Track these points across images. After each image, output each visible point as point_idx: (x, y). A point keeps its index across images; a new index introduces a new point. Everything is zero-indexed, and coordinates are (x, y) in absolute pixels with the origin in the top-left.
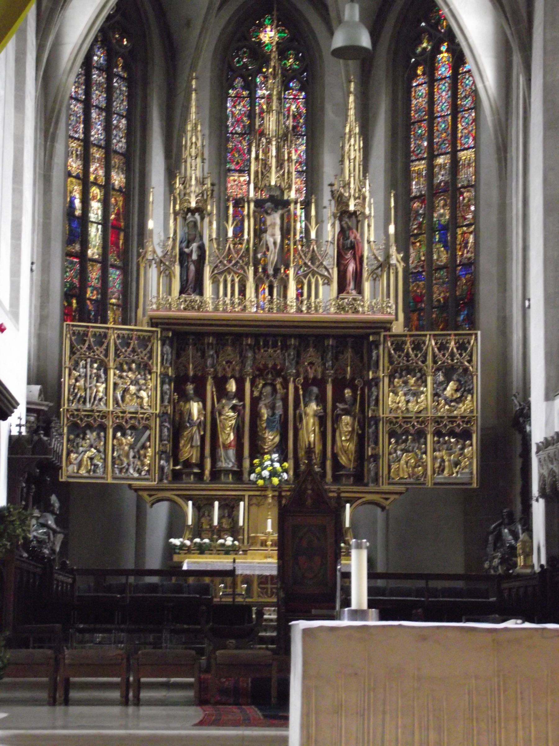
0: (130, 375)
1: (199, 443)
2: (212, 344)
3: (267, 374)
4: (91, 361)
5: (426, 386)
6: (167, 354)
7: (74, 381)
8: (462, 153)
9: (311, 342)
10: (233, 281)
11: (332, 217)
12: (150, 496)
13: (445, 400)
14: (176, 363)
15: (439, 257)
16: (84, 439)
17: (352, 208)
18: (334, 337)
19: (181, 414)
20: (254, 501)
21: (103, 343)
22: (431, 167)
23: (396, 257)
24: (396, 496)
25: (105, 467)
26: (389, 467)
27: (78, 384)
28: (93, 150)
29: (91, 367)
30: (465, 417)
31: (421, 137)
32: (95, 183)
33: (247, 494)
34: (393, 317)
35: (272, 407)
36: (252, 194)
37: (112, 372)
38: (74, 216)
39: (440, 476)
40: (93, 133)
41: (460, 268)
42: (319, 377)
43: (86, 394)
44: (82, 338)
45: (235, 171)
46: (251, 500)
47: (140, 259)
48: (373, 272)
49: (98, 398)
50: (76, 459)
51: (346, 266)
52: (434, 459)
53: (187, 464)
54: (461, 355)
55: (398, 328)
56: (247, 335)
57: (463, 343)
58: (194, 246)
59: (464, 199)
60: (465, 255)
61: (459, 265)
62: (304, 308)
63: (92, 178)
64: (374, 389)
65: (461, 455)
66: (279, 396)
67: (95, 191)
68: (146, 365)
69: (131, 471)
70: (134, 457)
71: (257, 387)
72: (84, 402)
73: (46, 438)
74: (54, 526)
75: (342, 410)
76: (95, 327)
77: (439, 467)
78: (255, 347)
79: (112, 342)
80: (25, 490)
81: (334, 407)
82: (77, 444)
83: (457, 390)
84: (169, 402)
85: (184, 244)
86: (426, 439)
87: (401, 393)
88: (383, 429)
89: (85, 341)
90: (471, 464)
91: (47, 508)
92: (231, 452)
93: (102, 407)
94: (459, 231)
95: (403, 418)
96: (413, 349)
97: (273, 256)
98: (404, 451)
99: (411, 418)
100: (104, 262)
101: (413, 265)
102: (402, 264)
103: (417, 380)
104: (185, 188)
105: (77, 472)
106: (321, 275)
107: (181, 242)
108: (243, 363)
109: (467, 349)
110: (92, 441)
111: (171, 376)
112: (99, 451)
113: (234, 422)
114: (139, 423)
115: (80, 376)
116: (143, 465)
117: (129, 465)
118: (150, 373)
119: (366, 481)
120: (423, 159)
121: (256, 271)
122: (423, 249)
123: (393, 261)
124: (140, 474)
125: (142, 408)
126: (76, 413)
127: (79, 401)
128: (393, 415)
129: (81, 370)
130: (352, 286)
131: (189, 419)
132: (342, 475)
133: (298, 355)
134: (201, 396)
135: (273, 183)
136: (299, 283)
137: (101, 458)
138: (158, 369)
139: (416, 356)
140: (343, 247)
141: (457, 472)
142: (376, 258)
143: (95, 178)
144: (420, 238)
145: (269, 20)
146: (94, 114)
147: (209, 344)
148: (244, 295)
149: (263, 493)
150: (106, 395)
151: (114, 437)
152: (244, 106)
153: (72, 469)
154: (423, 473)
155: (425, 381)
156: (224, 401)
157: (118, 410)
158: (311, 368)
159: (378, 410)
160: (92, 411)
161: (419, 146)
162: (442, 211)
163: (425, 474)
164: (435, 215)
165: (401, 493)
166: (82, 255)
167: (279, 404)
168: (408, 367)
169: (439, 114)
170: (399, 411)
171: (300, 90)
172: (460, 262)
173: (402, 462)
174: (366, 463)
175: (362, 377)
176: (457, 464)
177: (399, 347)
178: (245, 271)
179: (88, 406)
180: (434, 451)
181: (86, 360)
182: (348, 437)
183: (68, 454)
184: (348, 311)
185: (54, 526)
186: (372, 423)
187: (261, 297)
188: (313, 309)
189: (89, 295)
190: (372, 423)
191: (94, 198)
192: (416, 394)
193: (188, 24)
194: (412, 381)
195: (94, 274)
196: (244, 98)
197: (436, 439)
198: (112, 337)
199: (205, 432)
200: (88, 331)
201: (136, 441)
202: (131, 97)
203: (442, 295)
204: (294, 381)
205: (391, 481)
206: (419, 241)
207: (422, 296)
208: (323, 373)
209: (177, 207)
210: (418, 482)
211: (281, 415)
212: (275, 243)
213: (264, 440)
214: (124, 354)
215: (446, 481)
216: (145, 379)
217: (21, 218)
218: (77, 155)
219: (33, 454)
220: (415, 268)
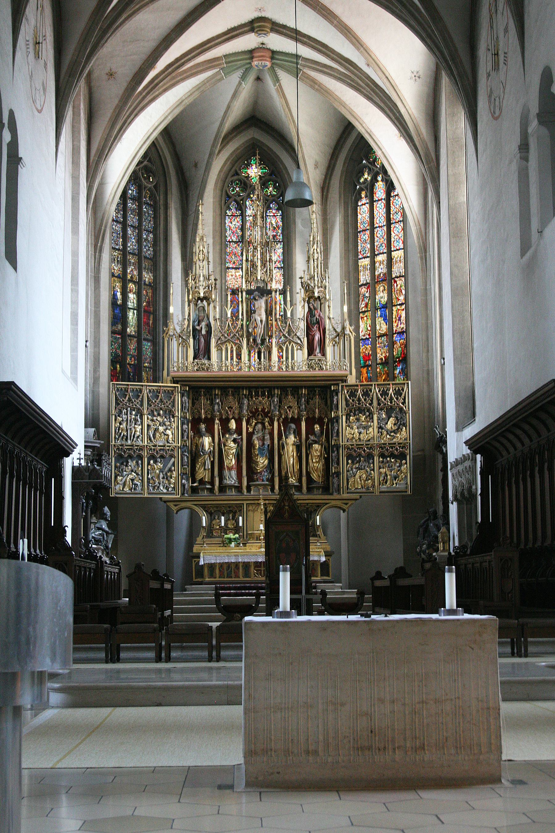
0: (159, 418)
1: (210, 467)
2: (218, 395)
3: (258, 415)
4: (131, 409)
5: (373, 422)
6: (186, 403)
7: (118, 424)
8: (395, 252)
9: (289, 392)
10: (232, 347)
11: (303, 301)
12: (176, 505)
13: (387, 432)
14: (192, 409)
15: (380, 327)
16: (126, 466)
17: (316, 295)
18: (305, 387)
19: (197, 446)
20: (250, 508)
21: (139, 396)
22: (373, 263)
23: (349, 329)
24: (353, 502)
25: (143, 486)
26: (348, 480)
27: (121, 426)
28: (130, 257)
29: (131, 414)
30: (401, 443)
32: (131, 281)
33: (245, 502)
34: (348, 372)
35: (263, 439)
36: (244, 287)
37: (146, 416)
38: (117, 305)
39: (384, 486)
40: (129, 245)
41: (395, 335)
42: (296, 417)
43: (127, 434)
44: (124, 392)
45: (233, 268)
46: (249, 506)
47: (165, 335)
48: (333, 339)
49: (136, 436)
50: (121, 480)
51: (314, 336)
52: (380, 473)
53: (202, 482)
54: (397, 399)
56: (243, 388)
57: (399, 389)
58: (203, 324)
59: (397, 285)
60: (399, 326)
61: (396, 333)
62: (284, 367)
63: (129, 277)
64: (335, 424)
65: (399, 471)
66: (267, 431)
67: (131, 286)
68: (170, 411)
69: (162, 488)
70: (163, 478)
71: (251, 425)
72: (126, 440)
73: (98, 468)
74: (107, 529)
75: (313, 441)
76: (133, 385)
77: (383, 480)
78: (249, 396)
79: (145, 395)
80: (85, 504)
81: (307, 438)
82: (122, 470)
83: (395, 424)
84: (188, 438)
85: (196, 323)
86: (373, 459)
87: (355, 427)
89: (126, 395)
90: (406, 477)
91: (102, 516)
92: (234, 473)
94: (394, 309)
95: (357, 445)
96: (362, 396)
97: (260, 331)
98: (359, 469)
99: (363, 445)
100: (139, 336)
101: (363, 333)
102: (354, 334)
103: (366, 417)
104: (195, 283)
105: (123, 490)
106: (295, 343)
107: (194, 322)
108: (241, 408)
109: (402, 394)
110: (133, 467)
111: (189, 419)
112: (137, 474)
113: (234, 451)
114: (166, 453)
115: (123, 420)
116: (170, 484)
117: (160, 484)
118: (173, 417)
119: (331, 490)
120: (368, 257)
121: (248, 340)
122: (369, 322)
123: (347, 332)
124: (168, 490)
125: (168, 442)
126: (120, 447)
127: (122, 438)
128: (349, 443)
129: (124, 416)
130: (318, 350)
131: (202, 449)
132: (313, 488)
133: (280, 401)
134: (210, 431)
135: (259, 278)
137: (140, 479)
138: (178, 413)
139: (365, 400)
140: (311, 322)
141: (396, 484)
142: (334, 329)
143: (131, 277)
144: (367, 314)
145: (254, 160)
147: (215, 395)
148: (240, 359)
149: (256, 502)
150: (142, 434)
151: (149, 464)
152: (238, 222)
153: (119, 487)
154: (372, 484)
155: (373, 418)
156: (227, 436)
157: (151, 444)
158: (289, 411)
159: (339, 440)
160: (132, 445)
161: (364, 248)
162: (382, 294)
163: (373, 486)
164: (377, 297)
165: (356, 499)
166: (123, 334)
167: (267, 437)
168: (359, 408)
169: (377, 225)
170: (354, 440)
171: (278, 210)
172: (396, 331)
173: (357, 476)
174: (331, 478)
175: (326, 416)
176: (395, 478)
177: (353, 394)
178: (240, 341)
179: (129, 442)
180: (380, 468)
181: (127, 409)
182: (317, 460)
183: (116, 477)
184: (315, 369)
185: (107, 529)
186: (335, 449)
187: (252, 359)
188: (290, 368)
189: (128, 360)
190: (335, 449)
191: (131, 291)
192: (366, 428)
193: (196, 165)
194: (363, 418)
195: (132, 346)
196: (238, 216)
197: (381, 459)
198: (145, 392)
199: (214, 458)
200: (128, 389)
201: (165, 466)
202: (156, 218)
203: (384, 355)
204: (278, 420)
205: (349, 491)
206: (366, 316)
207: (369, 355)
208: (298, 413)
209: (191, 297)
210: (368, 491)
211: (268, 445)
212: (261, 321)
213: (257, 463)
214: (154, 404)
215: (388, 490)
216: (170, 422)
217: (78, 309)
218: (118, 261)
219: (89, 479)
220: (364, 336)
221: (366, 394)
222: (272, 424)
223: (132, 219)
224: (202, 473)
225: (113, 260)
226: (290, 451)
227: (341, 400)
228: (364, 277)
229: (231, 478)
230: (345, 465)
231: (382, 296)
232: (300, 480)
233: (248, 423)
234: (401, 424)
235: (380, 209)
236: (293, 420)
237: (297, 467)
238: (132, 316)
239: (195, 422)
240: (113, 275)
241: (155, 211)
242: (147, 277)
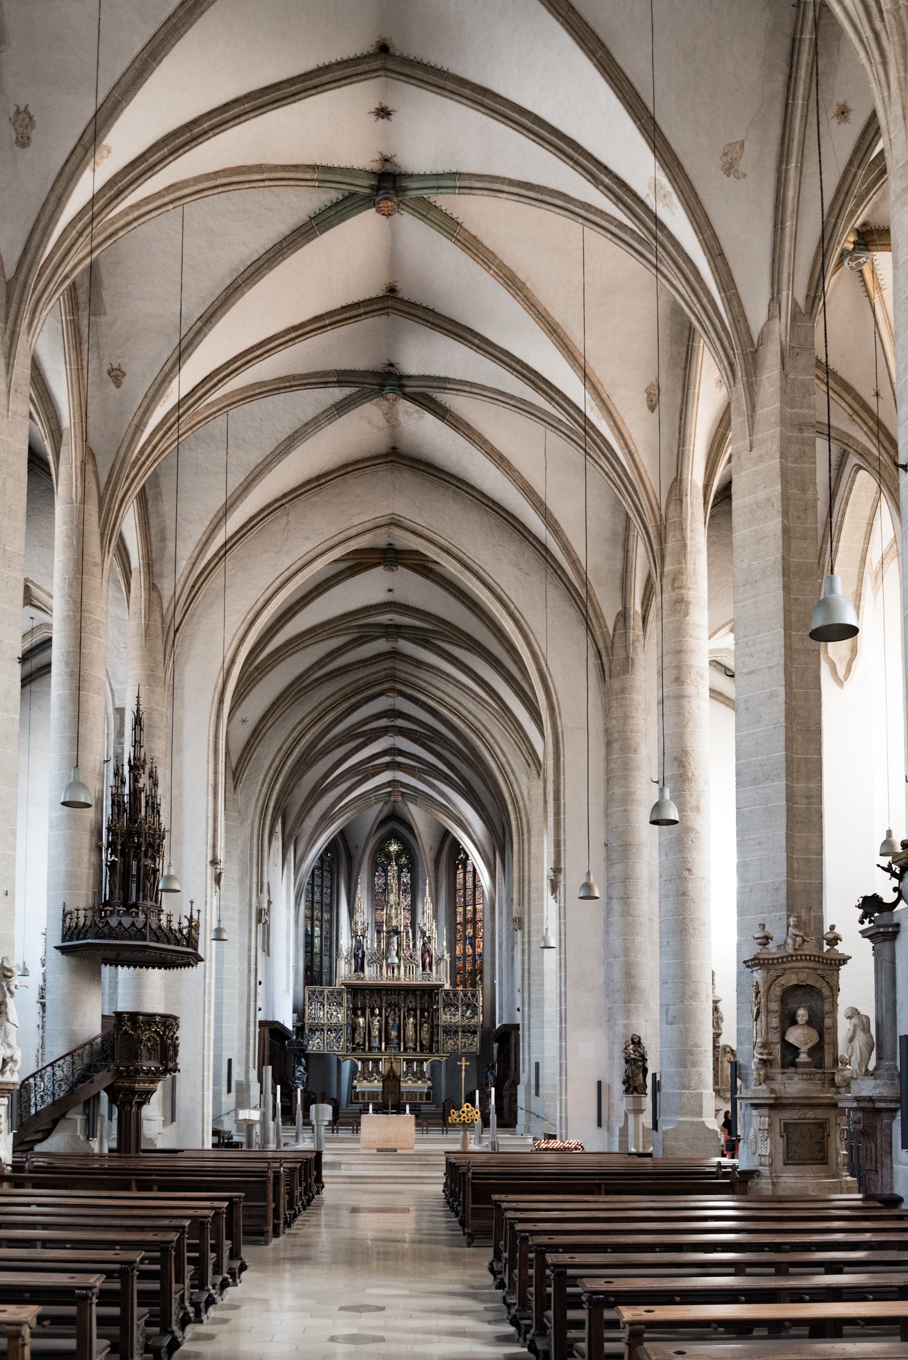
22: (465, 911)
23: (447, 956)
28: (315, 905)
31: (460, 897)
32: (317, 919)
35: (394, 1020)
44: (313, 992)
53: (358, 1044)
55: (447, 986)
58: (360, 951)
67: (317, 923)
76: (318, 988)
88: (441, 1030)
91: (300, 1064)
92: (377, 1039)
93: (322, 1021)
108: (381, 1001)
134: (364, 1015)
136: (406, 967)
138: (345, 1005)
146: (316, 889)
192: (454, 1015)
193: (357, 847)
195: (317, 960)
198: (326, 992)
202: (332, 879)
221: (455, 995)
222: (400, 1011)
223: (318, 881)
224: (359, 1039)
225: (306, 908)
226: (410, 1027)
227: (441, 997)
228: (459, 919)
229: (376, 1044)
230: (441, 1036)
231: (470, 932)
232: (416, 1045)
233: (386, 1010)
234: (475, 1013)
235: (469, 876)
236: (412, 1009)
237: (414, 1037)
238: (317, 941)
239: (354, 1010)
240: (306, 917)
241: (332, 875)
242: (326, 916)
